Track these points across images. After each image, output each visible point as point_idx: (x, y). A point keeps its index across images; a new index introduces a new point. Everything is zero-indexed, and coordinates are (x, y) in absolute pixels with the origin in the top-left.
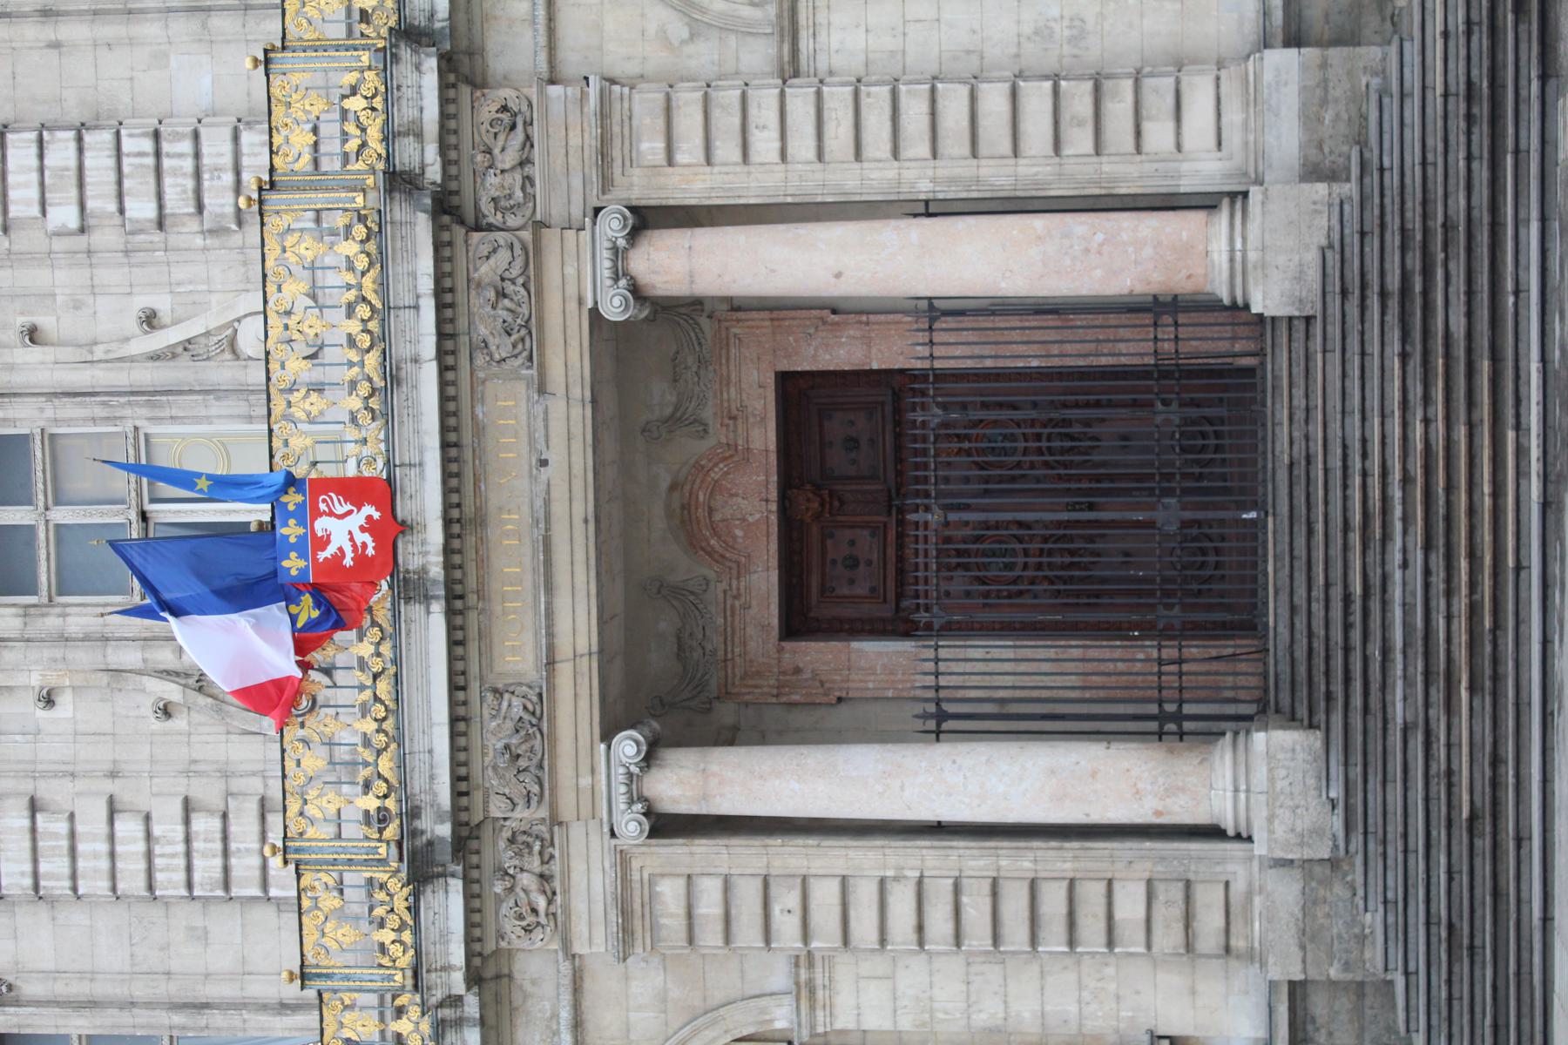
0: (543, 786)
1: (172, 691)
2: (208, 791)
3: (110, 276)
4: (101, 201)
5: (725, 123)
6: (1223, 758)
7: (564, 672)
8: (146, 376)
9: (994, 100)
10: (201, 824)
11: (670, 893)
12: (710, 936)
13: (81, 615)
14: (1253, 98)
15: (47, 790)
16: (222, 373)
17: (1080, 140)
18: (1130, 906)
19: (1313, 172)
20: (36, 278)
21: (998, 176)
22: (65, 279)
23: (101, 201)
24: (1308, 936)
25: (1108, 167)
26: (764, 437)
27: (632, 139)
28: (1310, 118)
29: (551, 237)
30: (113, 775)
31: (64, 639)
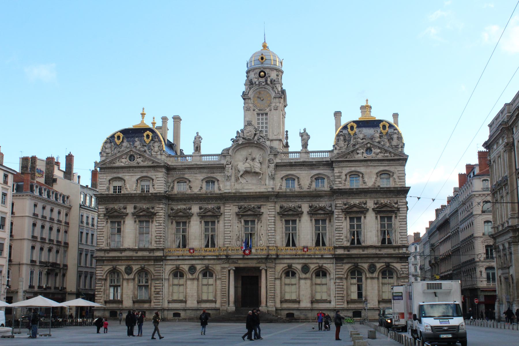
0: (231, 263)
1: (238, 235)
2: (231, 238)
3: (265, 232)
4: (270, 231)
5: (272, 275)
6: (233, 305)
7: (238, 265)
8: (258, 234)
9: (273, 292)
10: (229, 237)
11: (225, 271)
12: (222, 273)
13: (243, 229)
14: (272, 307)
15: (232, 226)
16: (259, 239)
17: (270, 297)
18: (224, 299)
19: (268, 311)
20: (265, 227)
21: (268, 292)
22: (265, 229)
23: (270, 231)
24: (223, 310)
25: (269, 298)
26: (254, 275)
27: (271, 269)
28: (271, 311)
29: (265, 264)
30: (233, 231)
31: (241, 228)
